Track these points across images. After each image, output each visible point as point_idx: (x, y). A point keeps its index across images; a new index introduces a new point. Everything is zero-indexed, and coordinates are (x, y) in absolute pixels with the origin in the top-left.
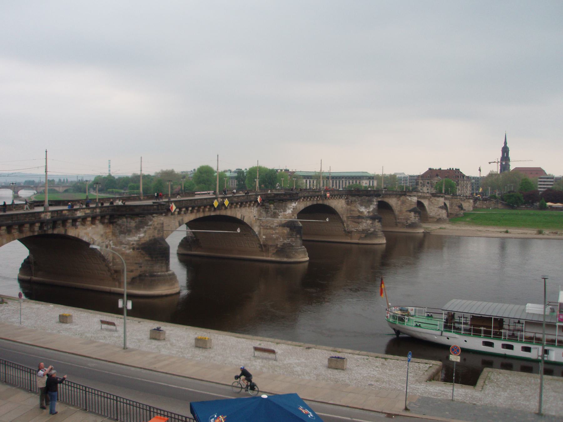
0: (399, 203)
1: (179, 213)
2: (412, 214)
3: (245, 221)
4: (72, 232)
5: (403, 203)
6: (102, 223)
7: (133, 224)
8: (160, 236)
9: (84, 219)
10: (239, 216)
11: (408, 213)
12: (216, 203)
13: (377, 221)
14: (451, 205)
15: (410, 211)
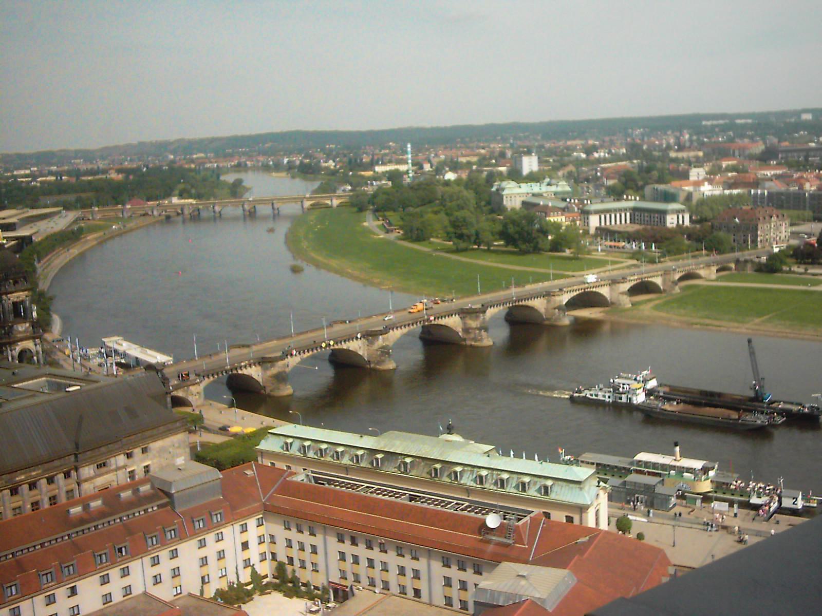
0: (545, 301)
1: (300, 354)
2: (557, 310)
3: (350, 349)
4: (240, 372)
5: (548, 302)
6: (255, 365)
7: (269, 365)
8: (283, 369)
9: (245, 367)
10: (345, 347)
11: (553, 311)
12: (324, 345)
13: (483, 331)
14: (664, 282)
15: (555, 308)
